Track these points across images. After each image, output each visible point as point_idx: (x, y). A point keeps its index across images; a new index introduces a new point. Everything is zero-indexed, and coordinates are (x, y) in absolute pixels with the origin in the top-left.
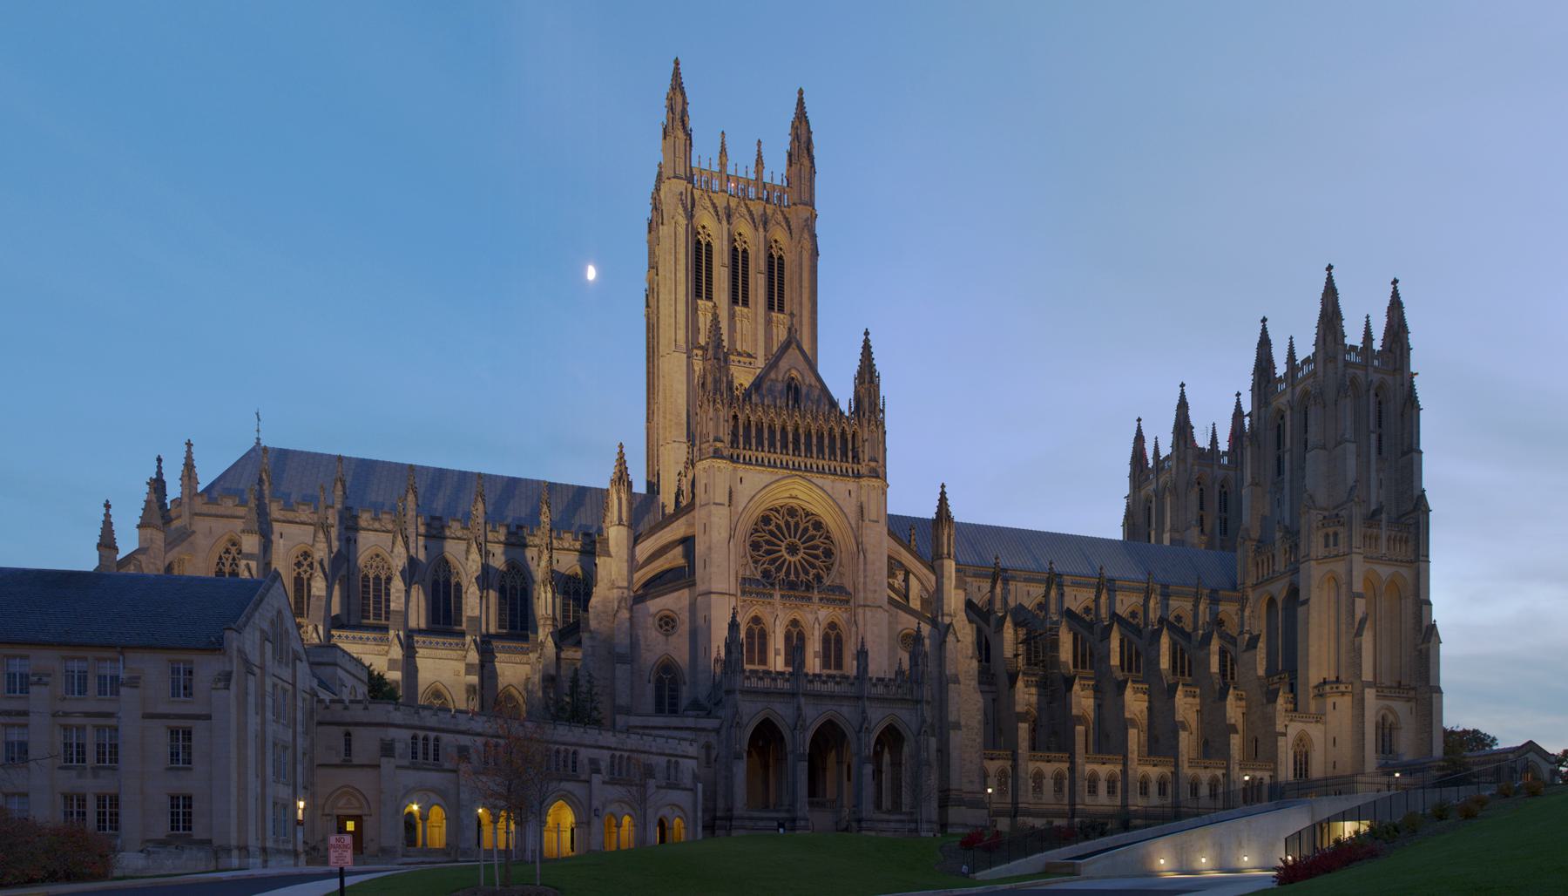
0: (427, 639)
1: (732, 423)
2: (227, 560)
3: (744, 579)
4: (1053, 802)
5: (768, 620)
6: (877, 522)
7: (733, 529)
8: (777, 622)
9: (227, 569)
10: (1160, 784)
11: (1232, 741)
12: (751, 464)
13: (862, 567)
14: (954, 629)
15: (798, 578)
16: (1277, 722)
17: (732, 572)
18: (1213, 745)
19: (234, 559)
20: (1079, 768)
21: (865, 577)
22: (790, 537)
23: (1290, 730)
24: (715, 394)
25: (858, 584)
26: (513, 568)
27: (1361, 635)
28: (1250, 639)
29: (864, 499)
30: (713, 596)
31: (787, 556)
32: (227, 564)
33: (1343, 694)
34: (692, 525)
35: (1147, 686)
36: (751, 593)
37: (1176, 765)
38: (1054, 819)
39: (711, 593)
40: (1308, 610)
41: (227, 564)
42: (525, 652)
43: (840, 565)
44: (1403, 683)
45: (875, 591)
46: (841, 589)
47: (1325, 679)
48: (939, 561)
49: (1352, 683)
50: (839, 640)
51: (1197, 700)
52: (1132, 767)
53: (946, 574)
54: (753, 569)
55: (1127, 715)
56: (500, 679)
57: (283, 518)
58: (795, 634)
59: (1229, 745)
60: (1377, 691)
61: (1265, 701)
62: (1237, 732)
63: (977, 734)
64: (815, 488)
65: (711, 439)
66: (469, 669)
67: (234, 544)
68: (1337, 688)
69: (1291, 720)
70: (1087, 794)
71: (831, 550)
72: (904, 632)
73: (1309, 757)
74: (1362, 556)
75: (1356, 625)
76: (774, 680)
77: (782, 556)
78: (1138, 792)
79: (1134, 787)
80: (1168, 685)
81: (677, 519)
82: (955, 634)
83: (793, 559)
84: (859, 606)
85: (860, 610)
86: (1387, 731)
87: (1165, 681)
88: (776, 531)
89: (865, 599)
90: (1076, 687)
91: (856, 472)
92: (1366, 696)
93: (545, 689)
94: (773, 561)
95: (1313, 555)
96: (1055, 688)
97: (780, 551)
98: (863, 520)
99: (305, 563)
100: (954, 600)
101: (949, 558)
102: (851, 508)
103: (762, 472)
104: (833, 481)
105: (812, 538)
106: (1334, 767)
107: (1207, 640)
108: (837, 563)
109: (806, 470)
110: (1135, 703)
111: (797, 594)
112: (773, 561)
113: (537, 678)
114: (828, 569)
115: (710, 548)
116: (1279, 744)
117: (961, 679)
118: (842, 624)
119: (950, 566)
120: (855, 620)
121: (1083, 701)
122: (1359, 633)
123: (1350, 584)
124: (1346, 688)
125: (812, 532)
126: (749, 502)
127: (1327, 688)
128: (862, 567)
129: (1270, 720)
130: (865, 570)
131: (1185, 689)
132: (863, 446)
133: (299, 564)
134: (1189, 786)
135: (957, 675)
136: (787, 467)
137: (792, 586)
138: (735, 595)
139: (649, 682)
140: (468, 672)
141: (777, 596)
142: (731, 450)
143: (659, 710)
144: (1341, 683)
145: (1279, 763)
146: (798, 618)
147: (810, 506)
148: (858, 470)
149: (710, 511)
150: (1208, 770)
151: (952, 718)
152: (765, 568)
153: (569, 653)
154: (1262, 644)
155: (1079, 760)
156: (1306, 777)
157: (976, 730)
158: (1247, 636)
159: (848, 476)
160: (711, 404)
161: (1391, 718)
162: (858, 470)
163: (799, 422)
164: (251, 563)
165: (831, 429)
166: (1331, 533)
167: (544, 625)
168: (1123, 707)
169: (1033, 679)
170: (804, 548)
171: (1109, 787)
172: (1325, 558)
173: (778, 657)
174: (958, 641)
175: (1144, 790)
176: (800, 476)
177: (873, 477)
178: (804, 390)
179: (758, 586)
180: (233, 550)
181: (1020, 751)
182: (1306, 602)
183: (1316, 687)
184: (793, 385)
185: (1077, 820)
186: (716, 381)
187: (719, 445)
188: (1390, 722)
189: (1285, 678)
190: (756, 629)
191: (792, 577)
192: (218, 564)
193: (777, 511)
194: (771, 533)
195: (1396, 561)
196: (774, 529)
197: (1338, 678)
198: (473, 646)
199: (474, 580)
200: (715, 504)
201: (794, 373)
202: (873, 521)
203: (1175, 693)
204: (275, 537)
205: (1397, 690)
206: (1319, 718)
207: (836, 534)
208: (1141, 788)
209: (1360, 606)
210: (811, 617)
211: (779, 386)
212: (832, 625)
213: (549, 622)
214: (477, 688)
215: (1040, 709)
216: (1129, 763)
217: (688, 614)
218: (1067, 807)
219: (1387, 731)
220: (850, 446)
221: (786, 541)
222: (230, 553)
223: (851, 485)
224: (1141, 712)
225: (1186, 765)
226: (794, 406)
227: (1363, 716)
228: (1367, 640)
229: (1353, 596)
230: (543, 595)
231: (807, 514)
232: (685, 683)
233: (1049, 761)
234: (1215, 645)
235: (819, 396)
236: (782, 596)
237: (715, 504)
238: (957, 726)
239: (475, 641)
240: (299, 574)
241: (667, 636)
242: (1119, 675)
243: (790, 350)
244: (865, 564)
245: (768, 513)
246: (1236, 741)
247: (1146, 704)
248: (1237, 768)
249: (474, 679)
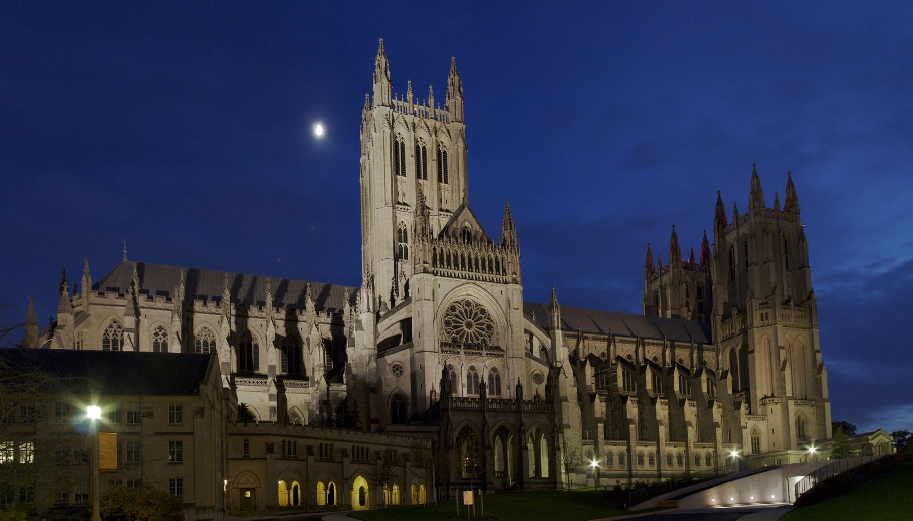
0: (243, 379)
1: (432, 252)
2: (111, 332)
3: (442, 343)
4: (618, 469)
5: (457, 367)
6: (518, 309)
7: (435, 313)
8: (463, 368)
9: (111, 338)
10: (678, 457)
11: (717, 432)
12: (445, 276)
14: (564, 371)
16: (741, 421)
17: (436, 339)
18: (706, 434)
19: (115, 331)
20: (633, 449)
21: (512, 341)
22: (468, 318)
23: (749, 424)
24: (423, 236)
25: (509, 345)
26: (290, 335)
27: (784, 370)
28: (722, 372)
29: (510, 296)
30: (425, 353)
31: (466, 329)
32: (111, 334)
33: (776, 404)
34: (410, 311)
35: (667, 401)
36: (447, 351)
37: (687, 446)
38: (620, 479)
39: (424, 351)
40: (754, 356)
41: (111, 334)
42: (306, 386)
43: (497, 334)
44: (808, 397)
45: (518, 349)
46: (498, 348)
47: (765, 395)
48: (553, 331)
49: (780, 398)
50: (498, 378)
51: (695, 409)
52: (663, 448)
53: (557, 338)
54: (447, 337)
55: (658, 418)
56: (288, 403)
57: (146, 306)
58: (473, 375)
59: (715, 434)
60: (795, 402)
61: (733, 408)
62: (719, 427)
63: (578, 431)
64: (481, 290)
65: (422, 262)
66: (271, 397)
67: (115, 322)
68: (773, 400)
69: (749, 419)
70: (638, 464)
71: (491, 325)
72: (535, 372)
73: (760, 440)
74: (782, 326)
75: (781, 365)
76: (463, 402)
78: (667, 462)
79: (664, 460)
80: (680, 400)
81: (402, 308)
82: (564, 373)
83: (469, 331)
84: (510, 358)
85: (510, 360)
86: (801, 424)
87: (678, 398)
88: (459, 315)
89: (513, 354)
90: (629, 402)
91: (505, 280)
92: (789, 405)
93: (321, 410)
94: (458, 332)
95: (755, 325)
96: (617, 403)
97: (462, 326)
98: (510, 308)
99: (161, 333)
100: (563, 354)
101: (559, 329)
102: (503, 303)
103: (451, 281)
104: (492, 286)
105: (480, 319)
106: (774, 446)
107: (699, 373)
108: (495, 333)
109: (476, 280)
110: (662, 411)
111: (474, 351)
113: (315, 402)
114: (490, 336)
115: (422, 325)
116: (743, 433)
117: (569, 399)
118: (499, 369)
119: (559, 334)
120: (507, 366)
121: (632, 410)
122: (783, 369)
123: (776, 341)
124: (778, 400)
125: (480, 315)
126: (445, 298)
127: (767, 400)
129: (737, 419)
130: (512, 337)
131: (690, 402)
132: (508, 265)
133: (156, 334)
134: (694, 458)
135: (566, 397)
136: (465, 278)
137: (468, 346)
138: (438, 352)
139: (388, 404)
140: (271, 400)
141: (462, 351)
142: (433, 268)
143: (394, 422)
144: (774, 397)
145: (744, 444)
146: (474, 365)
147: (478, 300)
148: (506, 280)
149: (422, 304)
150: (705, 449)
151: (564, 422)
153: (334, 387)
154: (730, 376)
155: (633, 444)
156: (759, 452)
157: (577, 429)
158: (721, 371)
159: (500, 283)
160: (421, 242)
161: (803, 417)
162: (506, 280)
163: (471, 252)
164: (130, 334)
165: (489, 256)
167: (319, 370)
168: (655, 413)
169: (603, 398)
170: (476, 325)
171: (650, 460)
172: (762, 326)
173: (464, 389)
174: (566, 377)
175: (670, 462)
176: (473, 283)
177: (515, 283)
178: (473, 234)
179: (450, 347)
180: (115, 326)
181: (599, 440)
182: (753, 351)
183: (761, 400)
184: (466, 231)
185: (634, 480)
186: (423, 229)
187: (426, 265)
188: (802, 419)
189: (743, 394)
191: (470, 342)
192: (105, 334)
193: (460, 303)
194: (457, 316)
195: (800, 328)
196: (458, 314)
197: (772, 395)
198: (273, 384)
199: (272, 343)
200: (425, 299)
201: (467, 224)
202: (516, 309)
203: (684, 404)
204: (141, 318)
205: (805, 401)
206: (764, 417)
207: (494, 316)
208: (668, 459)
209: (783, 354)
210: (482, 365)
211: (458, 232)
212: (494, 370)
213: (322, 369)
214: (277, 409)
215: (607, 415)
216: (661, 445)
217: (410, 364)
218: (627, 472)
219: (801, 424)
220: (501, 266)
221: (465, 321)
222: (112, 328)
223: (502, 287)
224: (665, 416)
225: (692, 446)
226: (468, 243)
227: (788, 415)
228: (788, 372)
229: (779, 348)
230: (318, 352)
231: (477, 305)
232: (408, 404)
233: (615, 445)
234: (704, 376)
235: (482, 237)
236: (465, 353)
237: (425, 299)
238: (568, 426)
239: (274, 380)
240: (156, 340)
241: (398, 377)
242: (652, 395)
243: (464, 211)
244: (512, 333)
245: (454, 304)
246: (719, 431)
247: (667, 411)
248: (721, 447)
249: (275, 404)
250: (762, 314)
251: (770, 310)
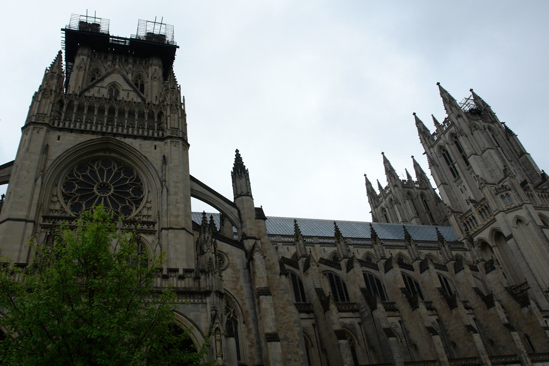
13: (165, 197)
128: (165, 197)
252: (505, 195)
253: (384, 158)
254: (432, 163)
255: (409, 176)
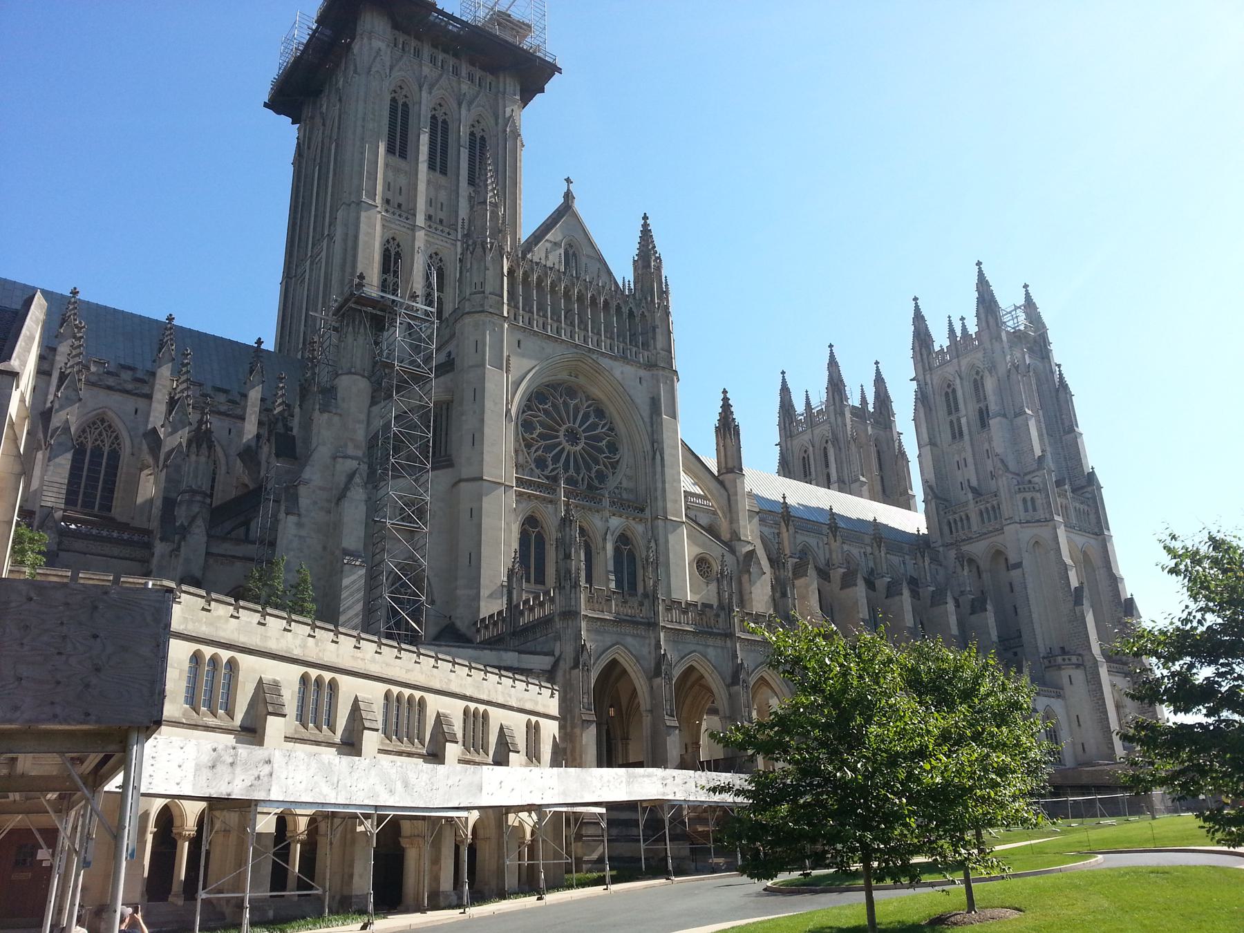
15: (578, 474)
77: (560, 444)
97: (557, 437)
112: (548, 449)
152: (539, 456)
166: (1029, 499)
190: (533, 533)
250: (1024, 500)
251: (1038, 494)
252: (1029, 499)
253: (832, 355)
254: (922, 398)
255: (863, 399)
